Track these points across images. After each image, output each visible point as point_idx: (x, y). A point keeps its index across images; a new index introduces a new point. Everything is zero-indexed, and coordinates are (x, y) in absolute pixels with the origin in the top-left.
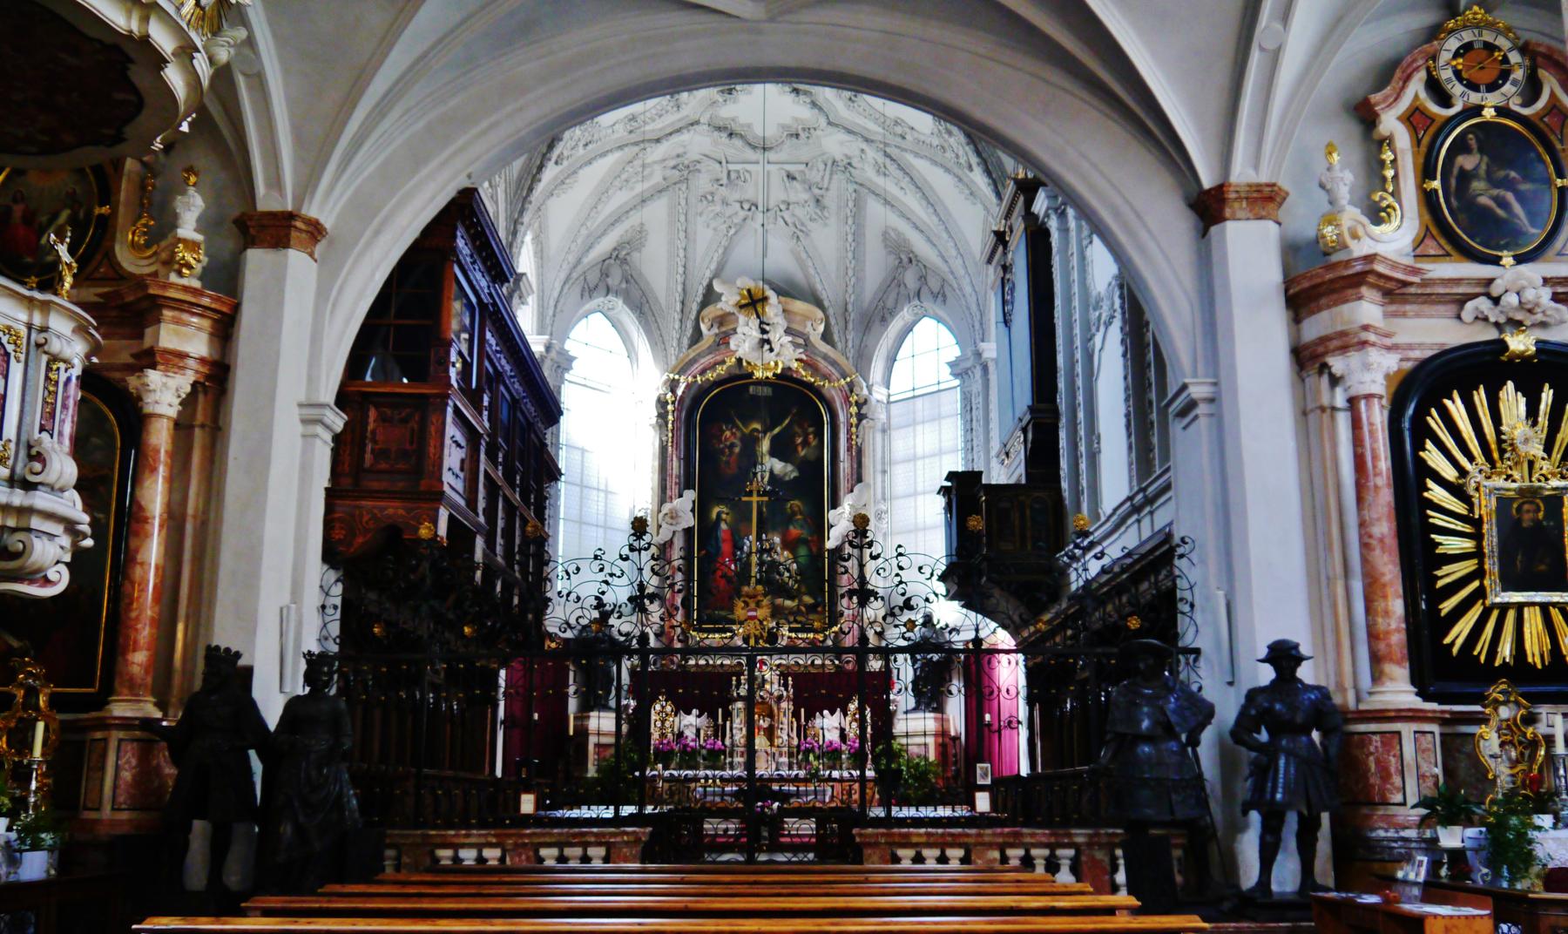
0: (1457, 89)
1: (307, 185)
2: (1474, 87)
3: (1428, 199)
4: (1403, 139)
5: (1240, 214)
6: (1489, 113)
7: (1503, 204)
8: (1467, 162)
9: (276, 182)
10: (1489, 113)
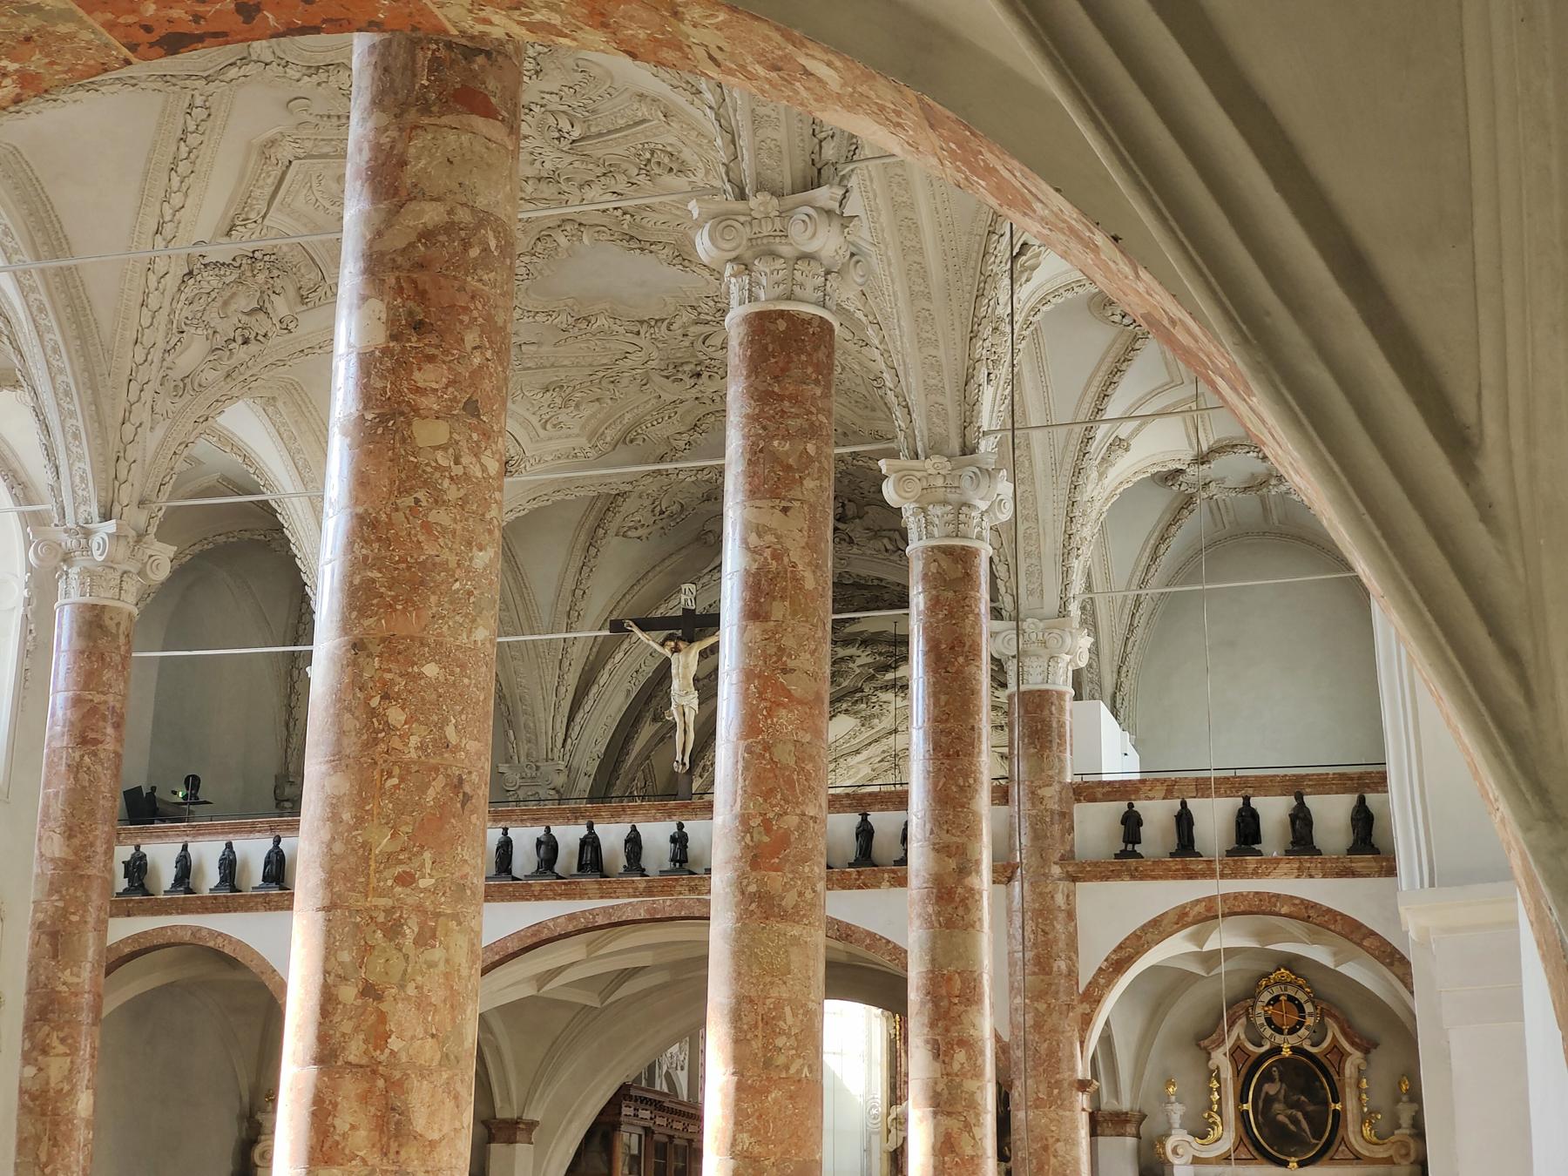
0: (1268, 1032)
1: (526, 1102)
2: (1279, 1031)
3: (1243, 1116)
4: (1227, 1072)
5: (1107, 1131)
6: (1286, 1053)
7: (1295, 1121)
8: (1271, 1089)
9: (507, 1098)
10: (1286, 1053)
